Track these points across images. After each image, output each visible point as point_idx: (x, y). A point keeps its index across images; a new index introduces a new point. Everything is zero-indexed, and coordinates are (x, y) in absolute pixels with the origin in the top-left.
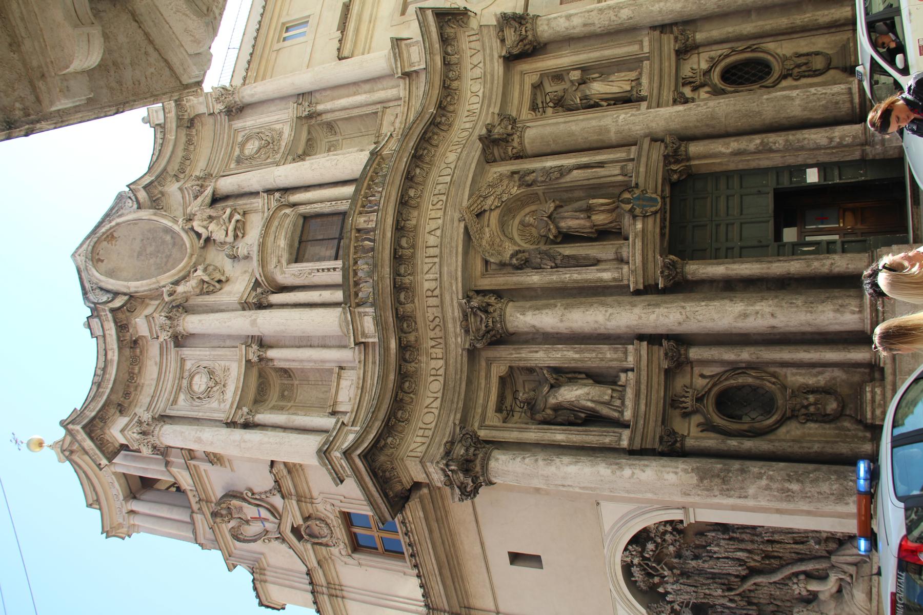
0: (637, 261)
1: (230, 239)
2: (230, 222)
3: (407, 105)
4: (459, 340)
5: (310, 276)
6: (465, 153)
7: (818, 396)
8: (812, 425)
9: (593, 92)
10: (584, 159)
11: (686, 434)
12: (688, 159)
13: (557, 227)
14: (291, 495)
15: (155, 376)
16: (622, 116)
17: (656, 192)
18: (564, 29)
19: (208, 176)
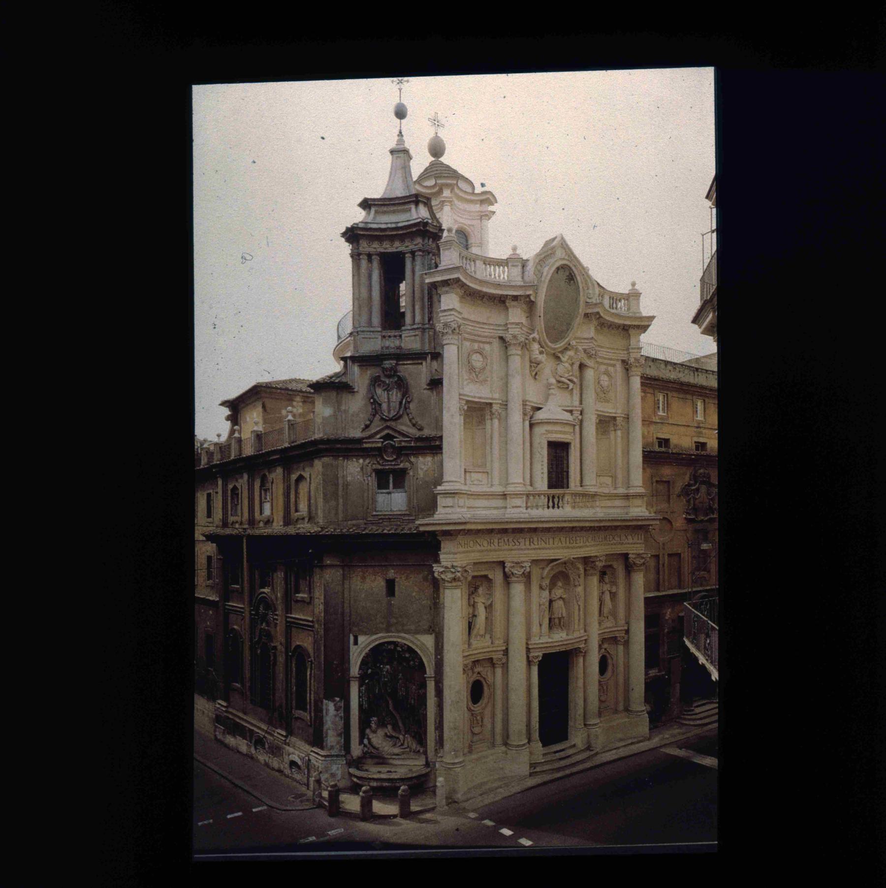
2: (569, 380)
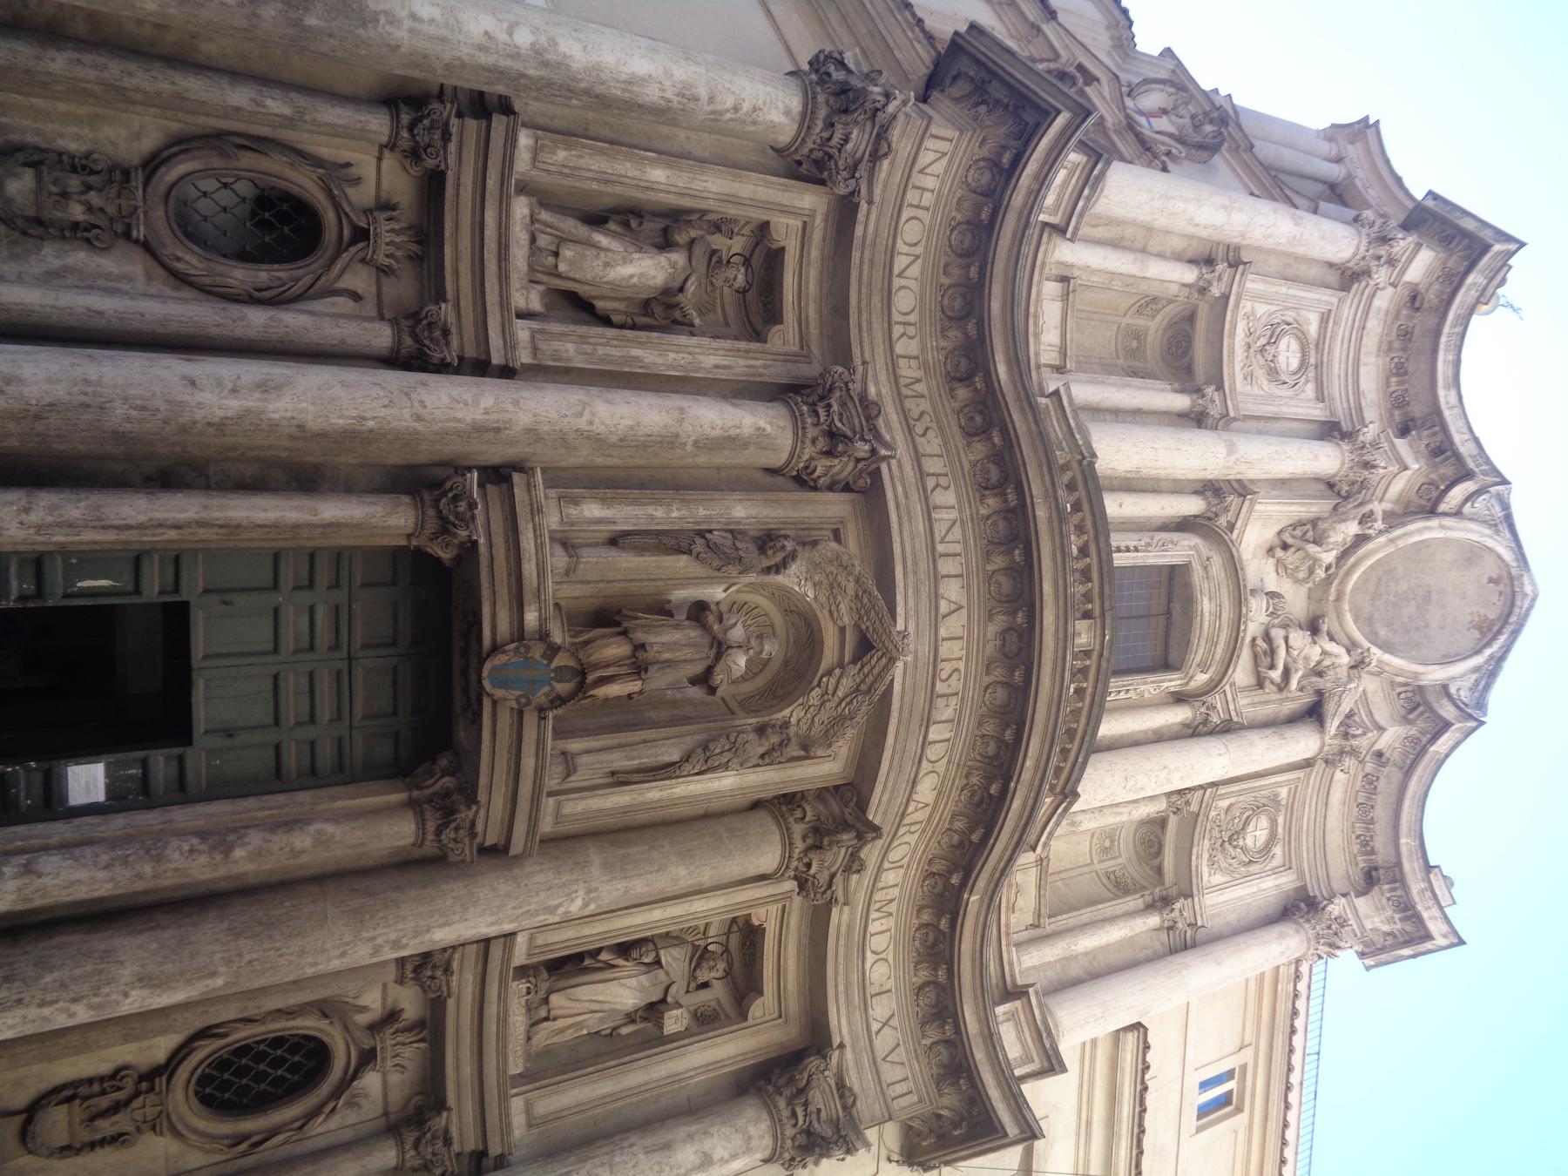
0: (531, 535)
1: (1278, 634)
3: (1003, 929)
5: (1148, 540)
6: (901, 798)
7: (59, 214)
8: (73, 146)
9: (633, 982)
10: (655, 793)
11: (387, 153)
12: (412, 804)
14: (1115, 131)
15: (1363, 370)
16: (579, 902)
17: (495, 703)
18: (713, 1130)
19: (1331, 761)
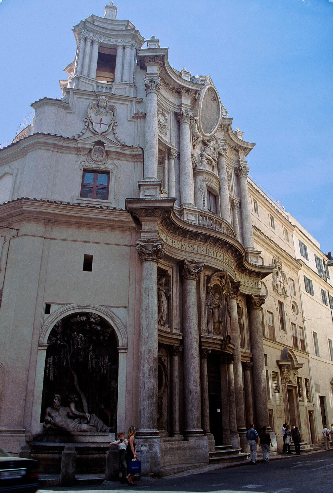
2: (213, 159)
4: (185, 257)
5: (201, 193)
13: (215, 308)
14: (123, 150)
